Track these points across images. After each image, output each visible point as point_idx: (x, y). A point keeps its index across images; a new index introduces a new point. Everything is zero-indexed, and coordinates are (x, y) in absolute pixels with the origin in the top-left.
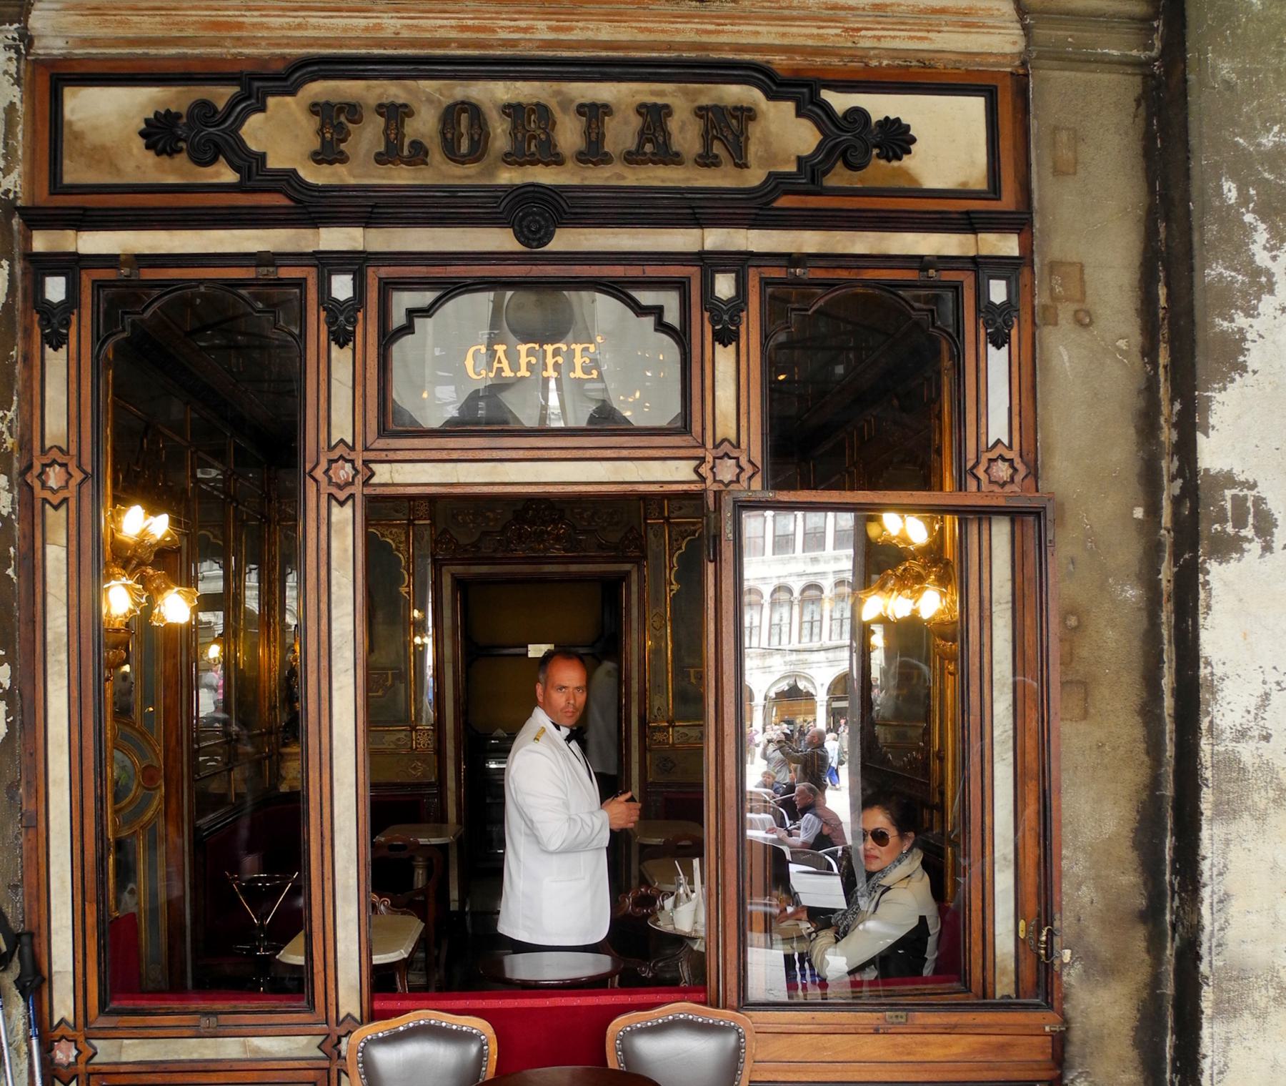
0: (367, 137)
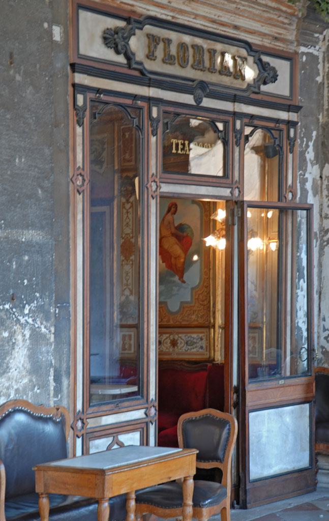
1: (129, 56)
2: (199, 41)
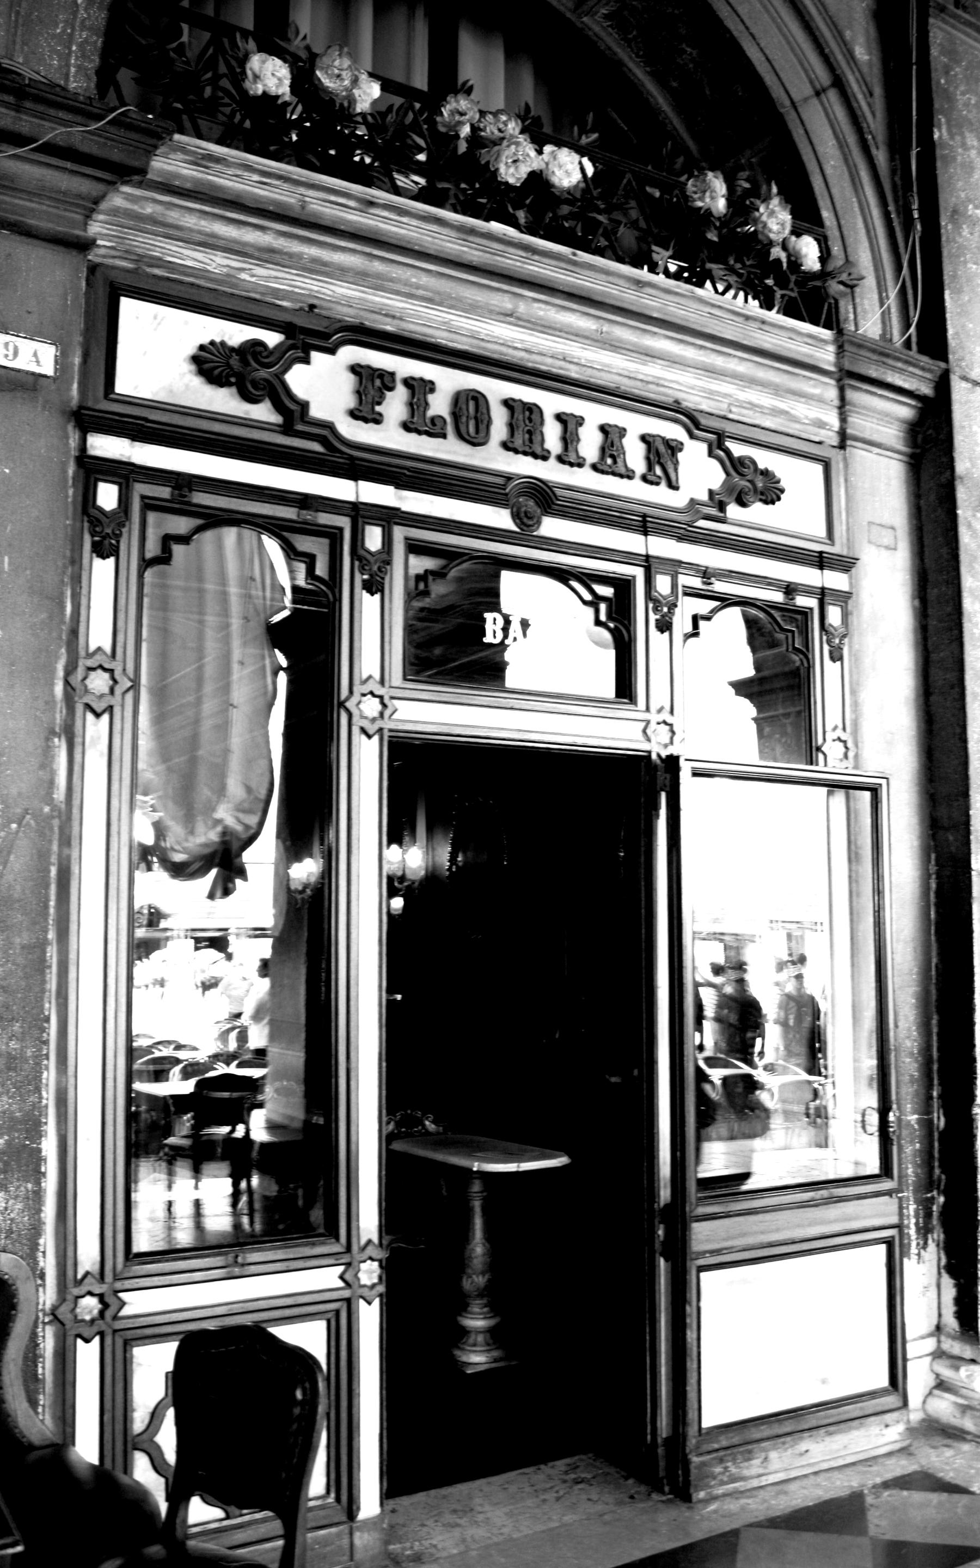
0: (395, 405)
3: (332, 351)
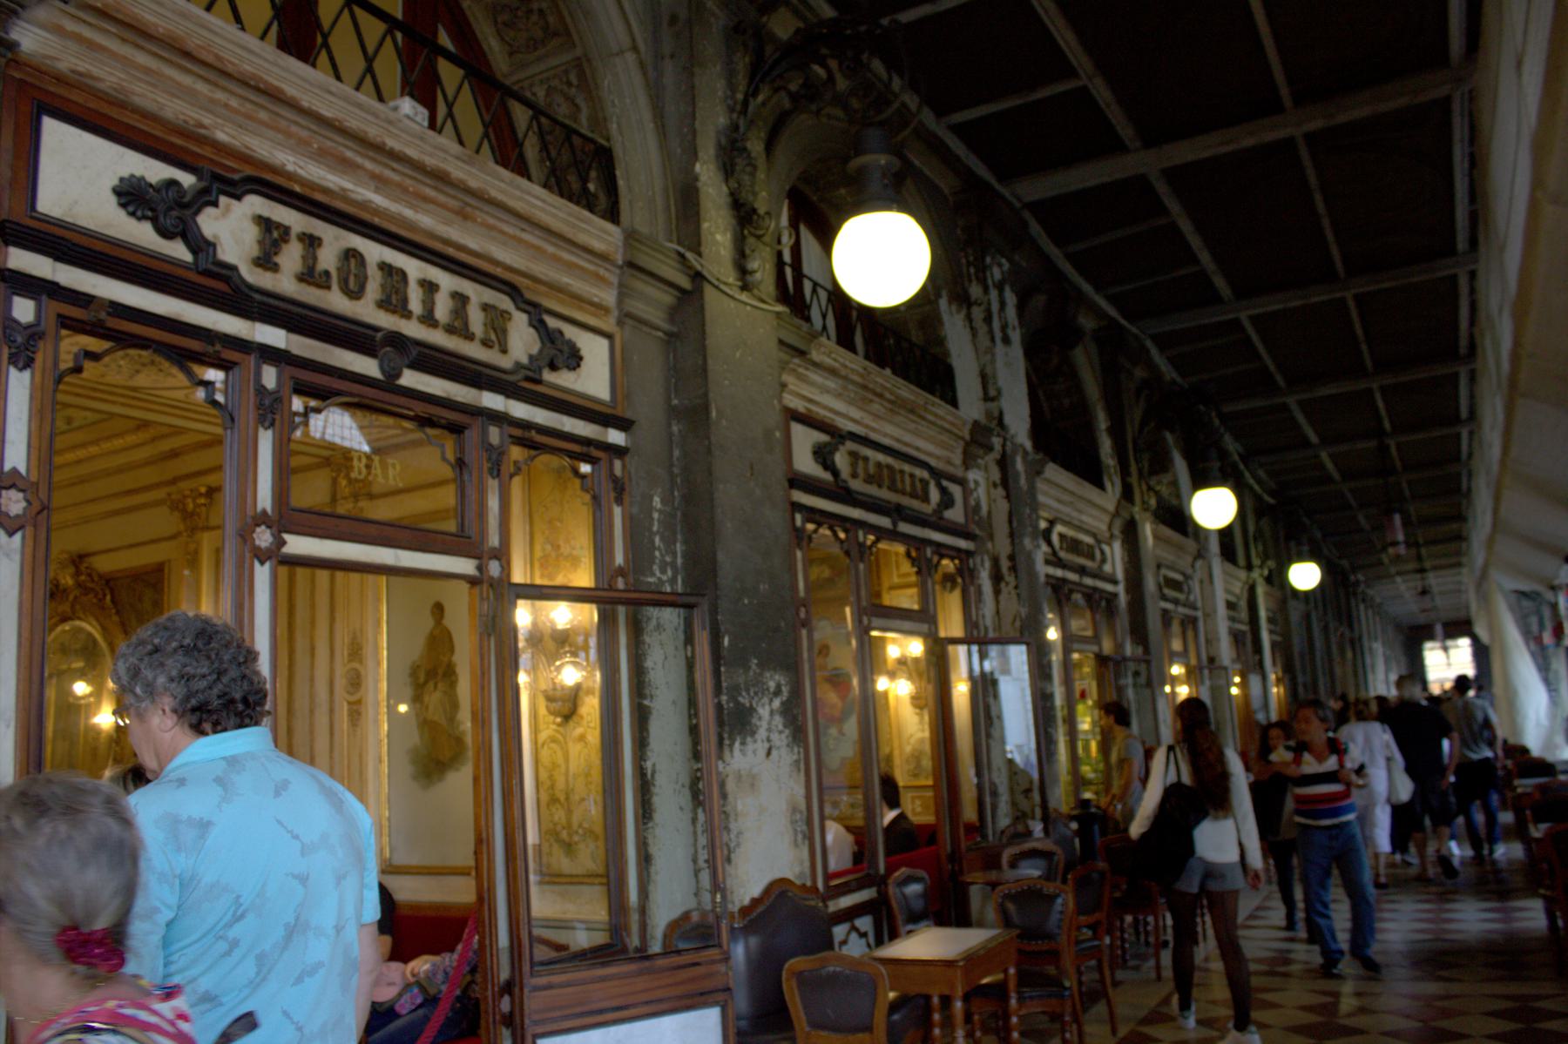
1: (835, 473)
2: (889, 460)
3: (238, 198)
